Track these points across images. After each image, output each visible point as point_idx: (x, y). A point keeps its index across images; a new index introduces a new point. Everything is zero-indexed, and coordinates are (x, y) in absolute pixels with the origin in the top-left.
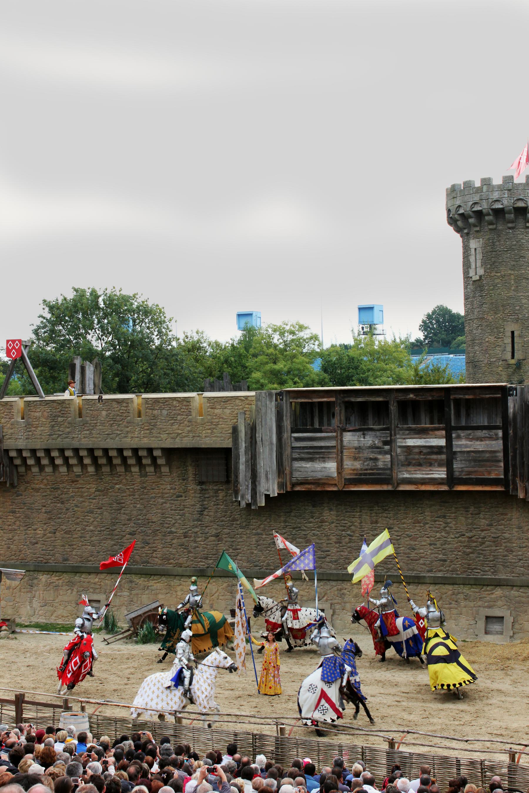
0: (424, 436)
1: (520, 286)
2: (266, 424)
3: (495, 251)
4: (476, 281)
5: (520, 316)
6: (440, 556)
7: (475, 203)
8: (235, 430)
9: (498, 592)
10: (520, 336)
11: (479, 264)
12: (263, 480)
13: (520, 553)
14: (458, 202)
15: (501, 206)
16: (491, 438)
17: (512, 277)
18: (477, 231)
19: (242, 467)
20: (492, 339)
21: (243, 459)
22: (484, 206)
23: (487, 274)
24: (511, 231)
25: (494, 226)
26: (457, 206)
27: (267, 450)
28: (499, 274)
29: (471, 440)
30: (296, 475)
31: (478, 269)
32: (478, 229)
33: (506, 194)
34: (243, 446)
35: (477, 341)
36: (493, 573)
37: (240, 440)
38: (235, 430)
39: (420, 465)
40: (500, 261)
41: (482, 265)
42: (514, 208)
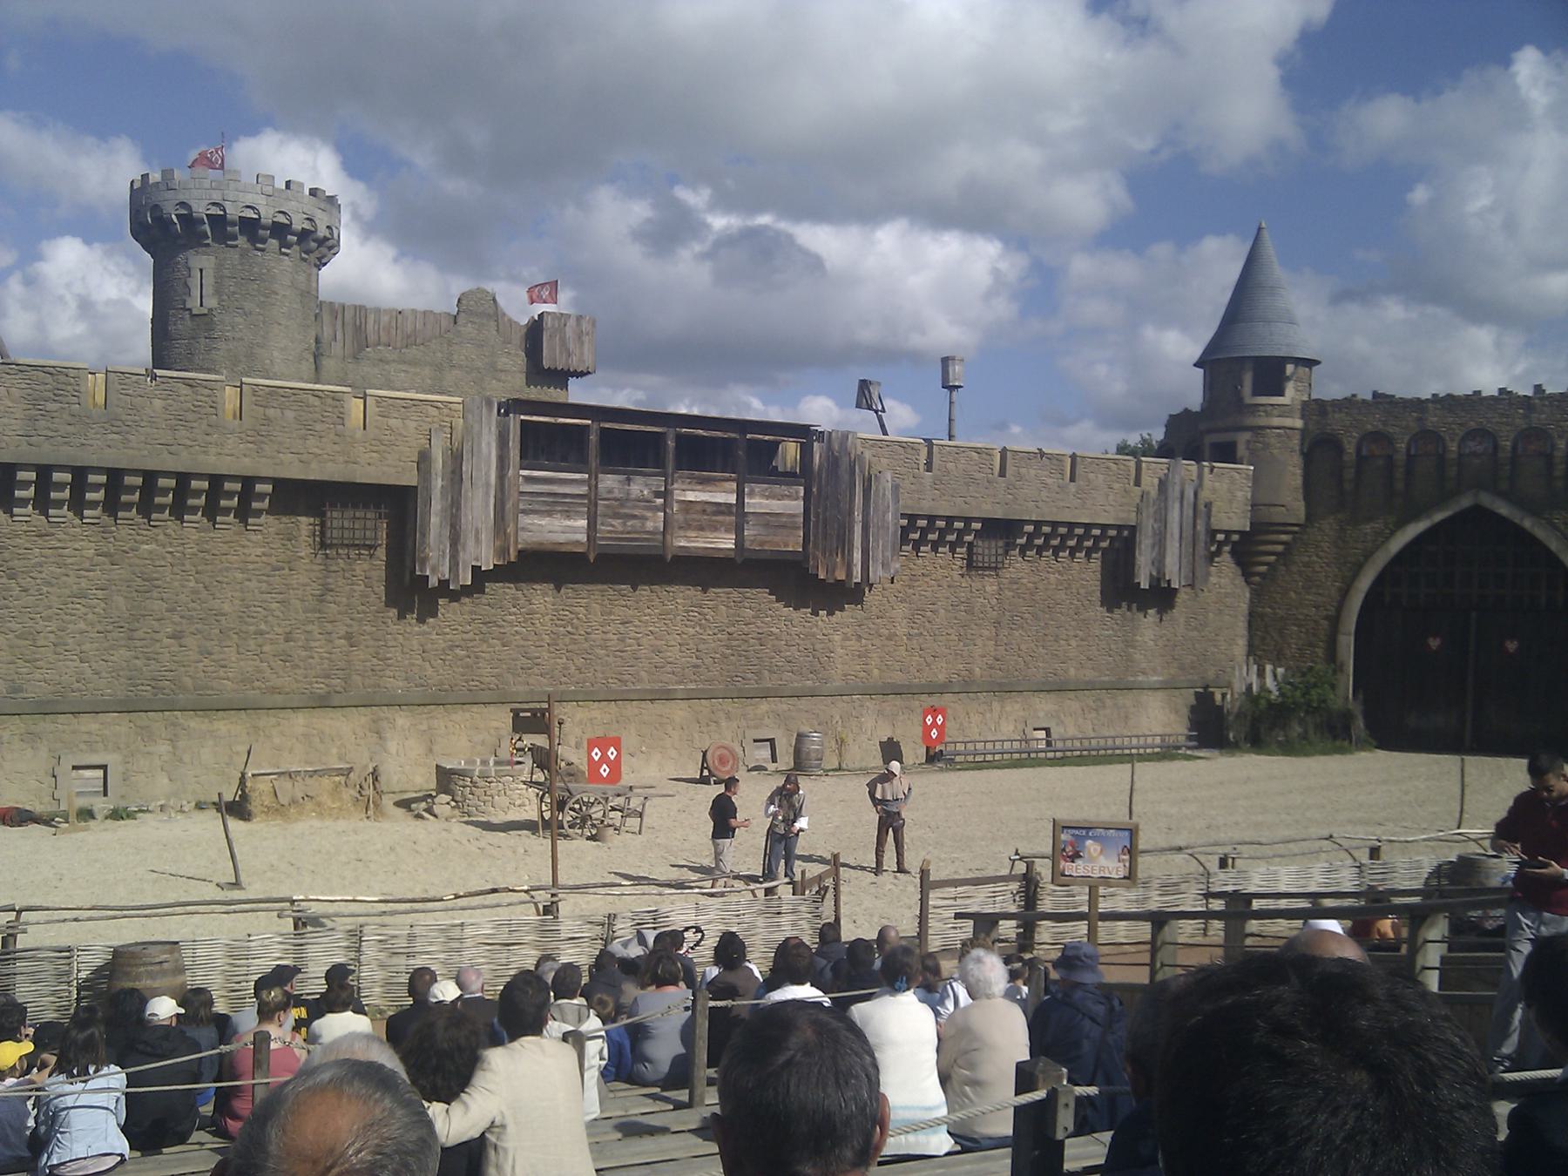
0: (709, 488)
2: (480, 451)
6: (694, 660)
8: (424, 459)
9: (764, 706)
12: (471, 543)
13: (788, 653)
16: (789, 497)
19: (435, 520)
21: (436, 505)
27: (480, 493)
29: (768, 498)
30: (523, 536)
34: (438, 483)
36: (756, 681)
37: (434, 476)
38: (424, 459)
39: (701, 528)
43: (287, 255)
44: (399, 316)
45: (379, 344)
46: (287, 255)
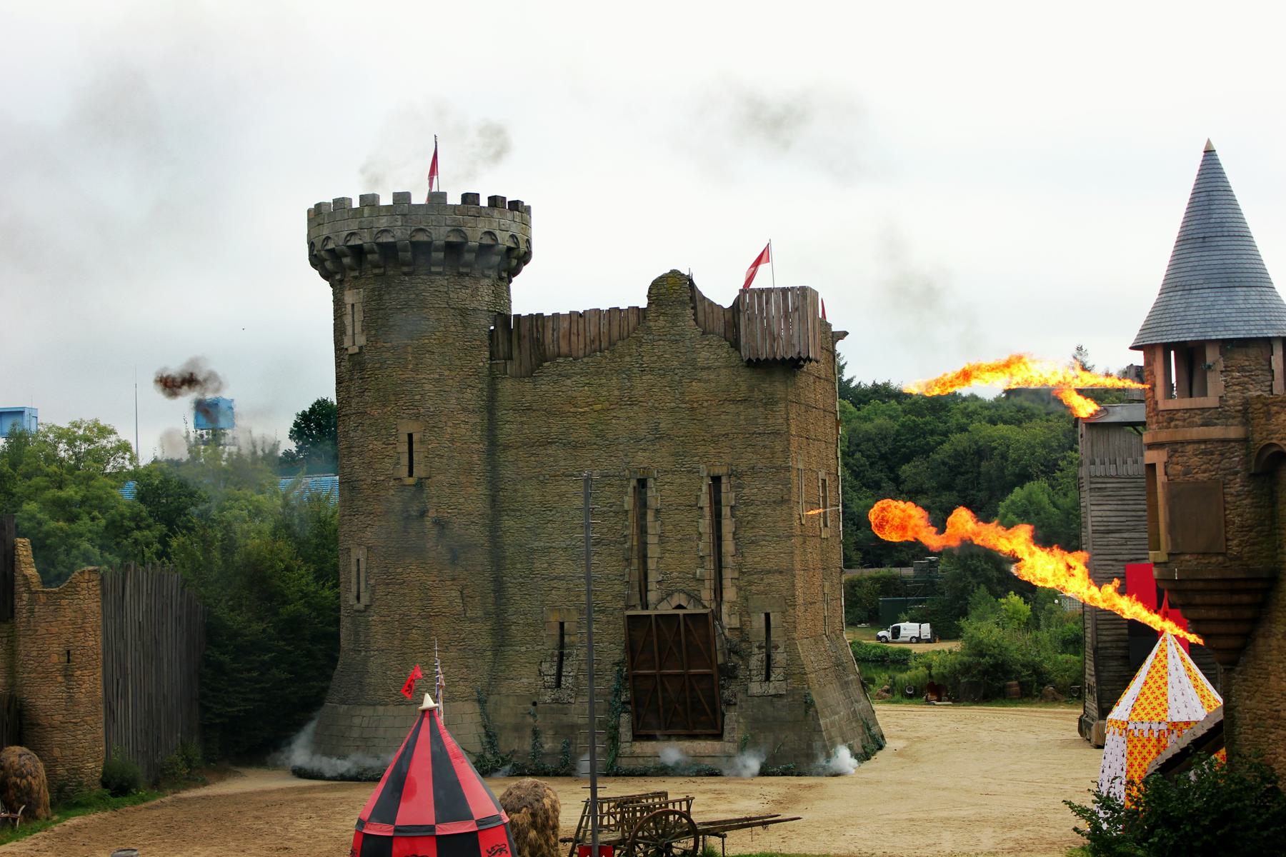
1: (421, 363)
3: (382, 309)
5: (422, 411)
7: (352, 234)
10: (422, 442)
11: (358, 328)
14: (325, 232)
15: (392, 240)
17: (410, 349)
18: (355, 278)
20: (379, 445)
22: (365, 239)
23: (370, 344)
24: (407, 278)
25: (382, 270)
26: (324, 237)
28: (388, 345)
31: (356, 337)
32: (357, 274)
33: (400, 220)
35: (356, 450)
40: (391, 323)
42: (412, 243)
43: (439, 273)
44: (581, 321)
45: (559, 356)
46: (439, 273)
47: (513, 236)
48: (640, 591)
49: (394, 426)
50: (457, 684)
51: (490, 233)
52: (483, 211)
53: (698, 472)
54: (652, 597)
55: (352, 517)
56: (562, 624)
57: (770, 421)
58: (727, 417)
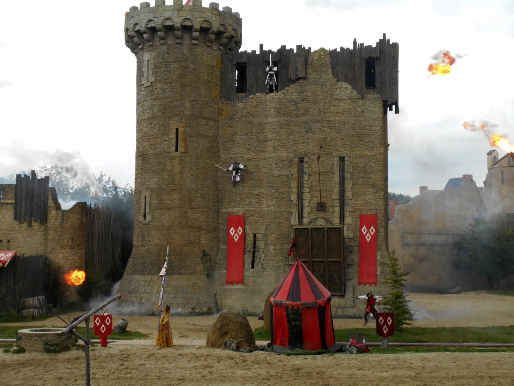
3: (164, 62)
4: (148, 87)
7: (150, 21)
11: (150, 72)
15: (171, 24)
18: (150, 46)
22: (158, 23)
31: (149, 77)
32: (151, 43)
35: (146, 138)
41: (153, 74)
42: (182, 25)
43: (196, 45)
47: (234, 30)
48: (299, 218)
49: (168, 124)
50: (198, 264)
51: (222, 25)
52: (220, 13)
53: (333, 155)
54: (306, 220)
55: (143, 174)
56: (255, 235)
57: (372, 128)
58: (349, 125)
